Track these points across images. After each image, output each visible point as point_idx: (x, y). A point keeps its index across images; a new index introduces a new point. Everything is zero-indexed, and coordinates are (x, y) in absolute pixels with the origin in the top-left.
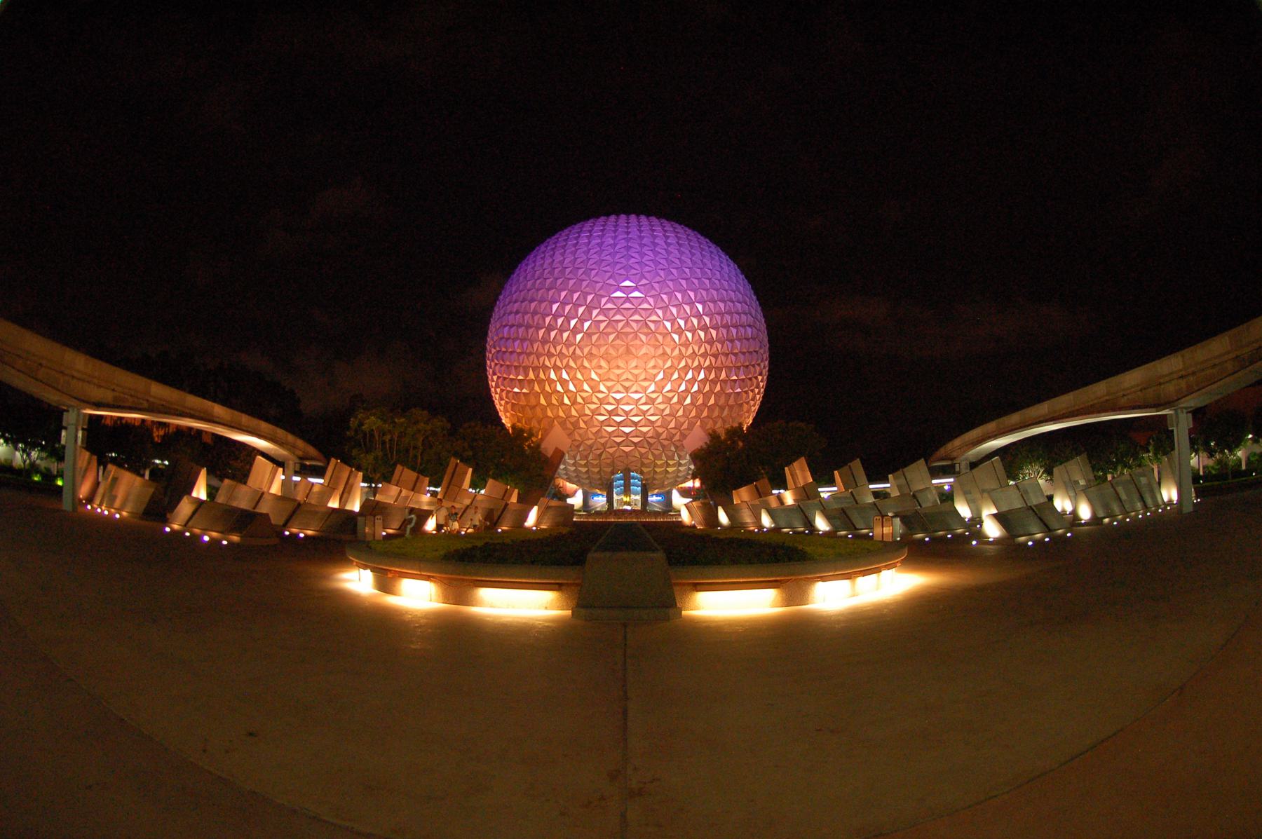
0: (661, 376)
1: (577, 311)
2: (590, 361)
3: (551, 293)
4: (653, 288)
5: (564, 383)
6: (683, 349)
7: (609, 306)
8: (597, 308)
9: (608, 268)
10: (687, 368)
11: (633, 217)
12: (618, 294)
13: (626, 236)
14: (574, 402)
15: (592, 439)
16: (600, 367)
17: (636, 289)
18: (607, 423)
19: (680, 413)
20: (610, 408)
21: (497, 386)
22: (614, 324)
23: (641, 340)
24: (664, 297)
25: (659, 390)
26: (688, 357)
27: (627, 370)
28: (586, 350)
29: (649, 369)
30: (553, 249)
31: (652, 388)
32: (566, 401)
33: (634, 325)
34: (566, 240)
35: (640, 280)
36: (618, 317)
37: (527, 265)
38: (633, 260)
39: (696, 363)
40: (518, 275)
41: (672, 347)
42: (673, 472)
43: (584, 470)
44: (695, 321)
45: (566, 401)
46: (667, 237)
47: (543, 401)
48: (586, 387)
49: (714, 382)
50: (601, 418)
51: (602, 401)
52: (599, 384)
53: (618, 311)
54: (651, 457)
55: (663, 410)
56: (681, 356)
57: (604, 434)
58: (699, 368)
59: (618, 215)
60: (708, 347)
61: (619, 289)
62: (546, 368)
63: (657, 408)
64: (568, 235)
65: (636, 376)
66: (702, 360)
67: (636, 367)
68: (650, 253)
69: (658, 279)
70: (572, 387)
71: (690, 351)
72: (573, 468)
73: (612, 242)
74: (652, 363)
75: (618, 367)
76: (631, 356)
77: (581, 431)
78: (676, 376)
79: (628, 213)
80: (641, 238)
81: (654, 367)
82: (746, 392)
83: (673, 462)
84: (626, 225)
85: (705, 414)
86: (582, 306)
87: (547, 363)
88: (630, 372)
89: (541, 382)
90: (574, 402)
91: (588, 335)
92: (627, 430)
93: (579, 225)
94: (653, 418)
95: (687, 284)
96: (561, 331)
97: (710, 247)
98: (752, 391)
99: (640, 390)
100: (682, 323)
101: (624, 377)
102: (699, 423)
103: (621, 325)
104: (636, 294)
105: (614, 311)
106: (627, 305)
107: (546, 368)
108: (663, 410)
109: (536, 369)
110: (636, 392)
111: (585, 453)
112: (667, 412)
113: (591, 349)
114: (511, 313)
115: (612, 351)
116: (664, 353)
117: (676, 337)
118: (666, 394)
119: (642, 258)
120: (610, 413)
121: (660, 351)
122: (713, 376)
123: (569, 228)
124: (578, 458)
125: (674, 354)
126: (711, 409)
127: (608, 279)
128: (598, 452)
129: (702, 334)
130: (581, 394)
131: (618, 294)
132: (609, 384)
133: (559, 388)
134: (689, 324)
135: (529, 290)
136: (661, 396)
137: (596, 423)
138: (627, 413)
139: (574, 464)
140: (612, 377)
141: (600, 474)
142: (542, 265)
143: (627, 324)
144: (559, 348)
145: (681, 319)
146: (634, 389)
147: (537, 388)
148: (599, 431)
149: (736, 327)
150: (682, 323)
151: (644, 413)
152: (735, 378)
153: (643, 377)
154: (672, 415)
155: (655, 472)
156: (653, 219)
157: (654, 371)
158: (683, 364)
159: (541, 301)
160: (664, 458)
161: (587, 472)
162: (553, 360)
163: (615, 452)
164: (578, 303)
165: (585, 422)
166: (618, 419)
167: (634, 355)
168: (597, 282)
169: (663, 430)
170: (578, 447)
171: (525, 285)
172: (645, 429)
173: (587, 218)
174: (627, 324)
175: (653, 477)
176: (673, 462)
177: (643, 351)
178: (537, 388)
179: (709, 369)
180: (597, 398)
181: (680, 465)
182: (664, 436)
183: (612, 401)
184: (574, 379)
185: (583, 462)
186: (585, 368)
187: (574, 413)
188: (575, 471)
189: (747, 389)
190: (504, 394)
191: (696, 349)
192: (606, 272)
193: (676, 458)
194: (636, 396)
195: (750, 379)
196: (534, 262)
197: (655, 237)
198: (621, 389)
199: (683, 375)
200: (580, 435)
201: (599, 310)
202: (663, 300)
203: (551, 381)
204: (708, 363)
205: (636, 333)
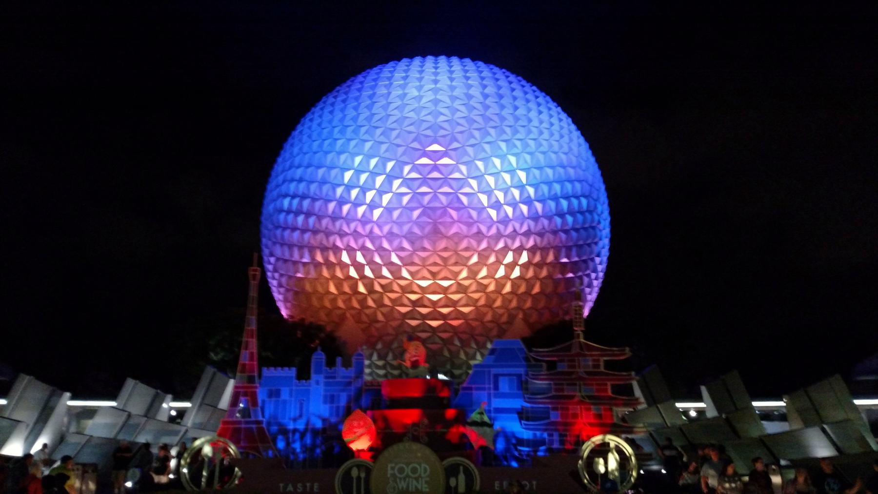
0: (475, 259)
2: (390, 242)
3: (343, 157)
4: (466, 153)
5: (359, 268)
6: (501, 227)
7: (414, 175)
8: (398, 178)
9: (411, 128)
10: (506, 249)
11: (442, 60)
13: (434, 86)
14: (371, 290)
16: (403, 249)
17: (445, 154)
18: (411, 315)
20: (414, 297)
21: (275, 270)
22: (419, 197)
23: (452, 217)
24: (480, 164)
25: (473, 274)
26: (508, 236)
27: (435, 252)
28: (386, 229)
29: (461, 250)
30: (344, 101)
31: (464, 274)
32: (362, 289)
33: (443, 199)
34: (359, 90)
35: (450, 144)
36: (424, 189)
37: (311, 120)
38: (442, 118)
39: (517, 244)
40: (301, 132)
41: (489, 224)
44: (516, 193)
45: (362, 289)
46: (485, 87)
48: (385, 272)
49: (539, 266)
50: (404, 310)
51: (406, 290)
53: (425, 181)
54: (463, 356)
56: (499, 236)
58: (520, 250)
59: (424, 56)
60: (532, 223)
62: (337, 250)
64: (361, 83)
65: (445, 260)
66: (524, 239)
67: (446, 249)
68: (463, 108)
69: (472, 141)
70: (368, 272)
71: (510, 229)
73: (415, 93)
74: (464, 244)
75: (424, 249)
77: (378, 325)
78: (492, 259)
79: (436, 54)
80: (452, 88)
81: (467, 249)
82: (580, 278)
84: (434, 70)
85: (528, 304)
86: (380, 174)
87: (339, 243)
88: (438, 255)
89: (330, 265)
90: (371, 290)
91: (389, 210)
92: (434, 323)
93: (375, 70)
95: (507, 146)
96: (356, 205)
97: (537, 97)
98: (588, 276)
99: (450, 276)
101: (431, 261)
102: (521, 316)
103: (427, 199)
104: (446, 161)
105: (420, 181)
106: (435, 175)
107: (337, 250)
108: (477, 300)
109: (324, 249)
110: (446, 278)
113: (391, 228)
114: (292, 180)
115: (416, 230)
116: (479, 232)
117: (493, 213)
118: (481, 281)
119: (453, 115)
120: (415, 303)
121: (474, 230)
123: (364, 74)
125: (490, 234)
126: (535, 298)
127: (412, 142)
129: (524, 208)
130: (379, 280)
131: (425, 161)
132: (413, 269)
133: (353, 273)
134: (509, 197)
135: (315, 153)
137: (396, 315)
138: (434, 304)
140: (417, 260)
142: (330, 122)
143: (435, 197)
144: (353, 225)
146: (442, 275)
148: (400, 326)
149: (567, 198)
150: (500, 196)
151: (454, 304)
152: (565, 260)
153: (452, 261)
154: (489, 305)
156: (467, 61)
157: (466, 254)
158: (501, 245)
159: (331, 168)
161: (385, 376)
162: (345, 239)
164: (376, 171)
167: (443, 235)
168: (399, 146)
169: (477, 323)
171: (310, 146)
172: (455, 323)
173: (386, 61)
174: (435, 197)
177: (454, 230)
178: (325, 273)
179: (532, 251)
180: (399, 285)
183: (416, 289)
184: (371, 263)
185: (380, 363)
186: (385, 250)
187: (370, 303)
189: (580, 274)
190: (284, 280)
191: (517, 226)
192: (410, 132)
194: (445, 283)
195: (585, 261)
196: (320, 116)
197: (469, 87)
198: (428, 275)
199: (501, 257)
202: (477, 168)
203: (344, 266)
204: (531, 243)
205: (444, 208)
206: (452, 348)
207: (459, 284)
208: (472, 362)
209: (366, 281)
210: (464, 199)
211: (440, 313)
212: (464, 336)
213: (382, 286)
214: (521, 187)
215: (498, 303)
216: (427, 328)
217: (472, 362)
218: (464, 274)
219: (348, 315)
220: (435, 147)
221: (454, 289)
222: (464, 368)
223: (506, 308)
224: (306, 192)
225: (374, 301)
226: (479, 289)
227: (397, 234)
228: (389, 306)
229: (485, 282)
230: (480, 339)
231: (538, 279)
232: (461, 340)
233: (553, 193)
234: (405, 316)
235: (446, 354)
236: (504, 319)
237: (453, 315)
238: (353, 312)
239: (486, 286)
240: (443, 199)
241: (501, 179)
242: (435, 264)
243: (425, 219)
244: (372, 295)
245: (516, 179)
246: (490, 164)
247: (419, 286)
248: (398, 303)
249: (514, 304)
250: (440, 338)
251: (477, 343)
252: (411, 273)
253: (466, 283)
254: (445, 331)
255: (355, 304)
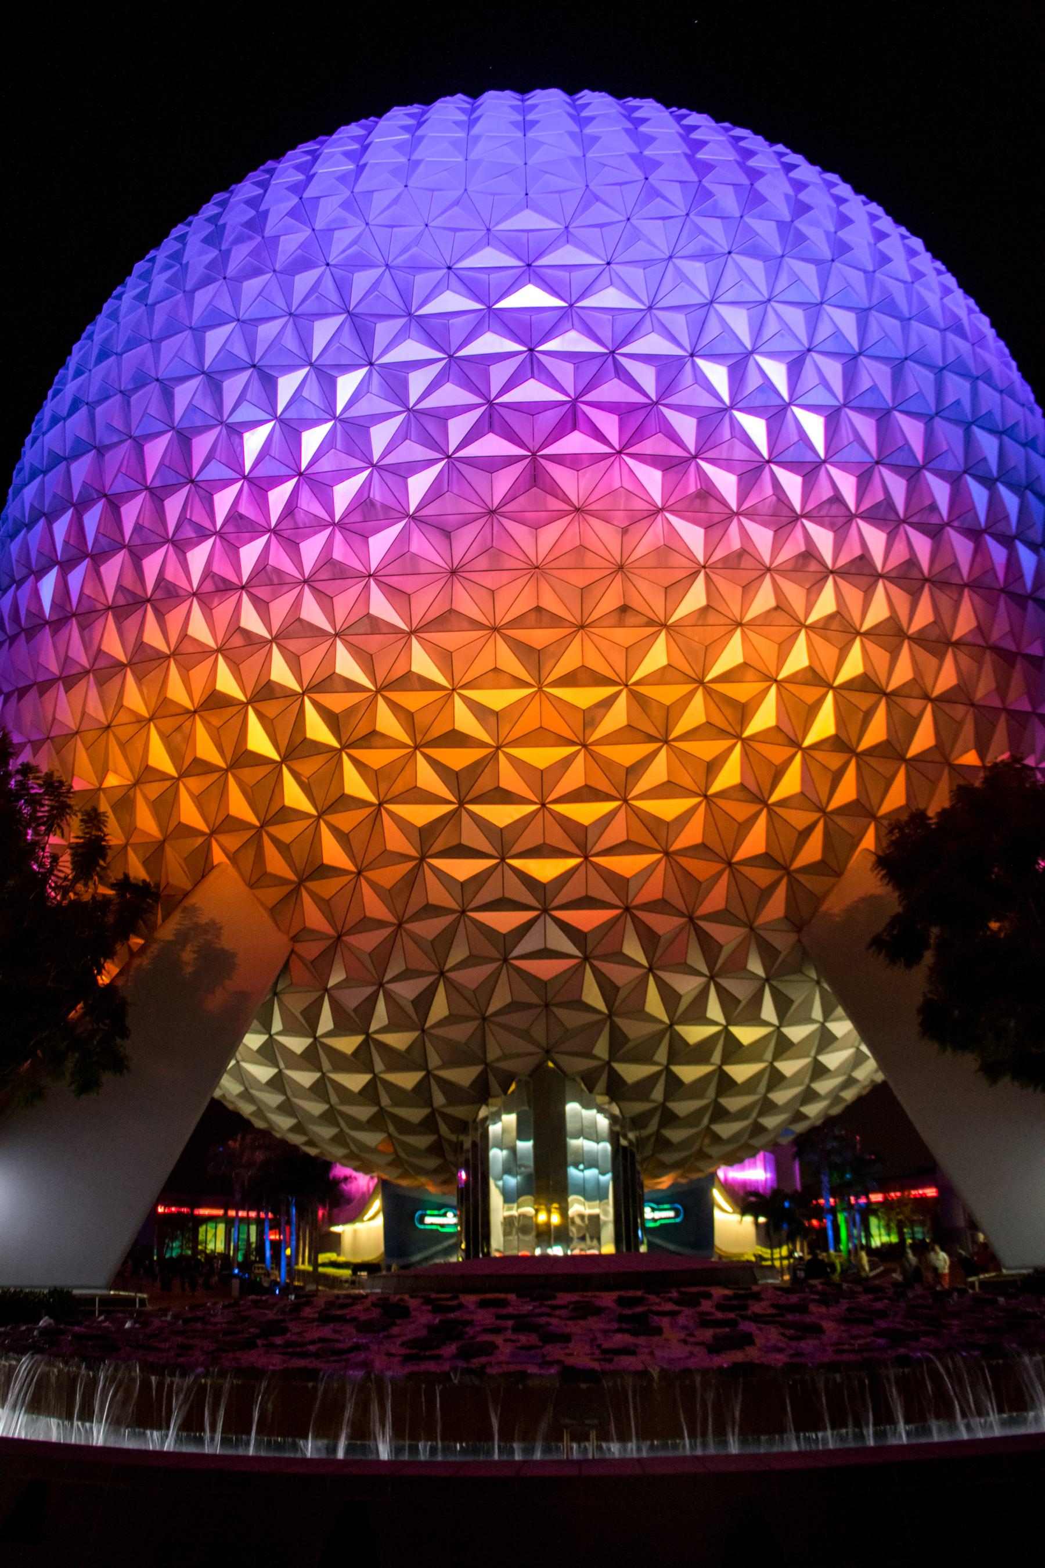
1: (305, 341)
12: (490, 257)
15: (381, 924)
17: (567, 236)
19: (790, 784)
20: (458, 759)
42: (751, 1084)
43: (355, 1082)
44: (833, 370)
45: (259, 741)
47: (160, 758)
48: (346, 665)
52: (408, 645)
54: (654, 1004)
55: (712, 768)
57: (438, 894)
61: (489, 238)
63: (683, 756)
72: (306, 1078)
76: (555, 504)
77: (328, 888)
83: (761, 1032)
94: (668, 809)
100: (777, 373)
102: (869, 841)
111: (353, 999)
112: (729, 775)
118: (721, 688)
122: (923, 616)
124: (326, 1022)
128: (407, 991)
131: (490, 257)
136: (699, 697)
137: (396, 841)
139: (310, 1059)
141: (429, 1103)
145: (771, 355)
147: (134, 699)
148: (412, 880)
155: (674, 1084)
160: (714, 1010)
161: (369, 1093)
163: (490, 985)
165: (343, 838)
166: (501, 815)
167: (566, 500)
170: (321, 966)
175: (664, 1107)
176: (761, 1032)
181: (784, 1047)
182: (716, 899)
185: (347, 1044)
187: (294, 795)
188: (319, 1090)
193: (768, 1011)
198: (511, 664)
200: (324, 905)
201: (402, 321)
206: (620, 974)
207: (639, 700)
208: (694, 1034)
209: (272, 709)
210: (646, 377)
211: (564, 821)
212: (663, 924)
213: (332, 720)
214: (851, 362)
215: (790, 784)
216: (518, 892)
217: (694, 1034)
218: (657, 657)
219: (218, 856)
220: (528, 220)
221: (617, 717)
222: (661, 1054)
223: (822, 810)
224: (83, 436)
225: (306, 788)
226: (719, 721)
227: (386, 508)
228: (365, 804)
229: (740, 692)
230: (727, 936)
231: (927, 697)
232: (649, 939)
233: (949, 399)
234: (426, 835)
235: (593, 995)
236: (812, 851)
237: (616, 833)
238: (233, 842)
239: (744, 711)
240: (565, 372)
241: (771, 317)
242: (540, 615)
243: (492, 445)
244: (297, 766)
245: (824, 331)
246: (730, 277)
247: (479, 711)
248: (399, 787)
249: (847, 791)
250: (568, 930)
251: (709, 947)
252: (445, 658)
253: (667, 694)
254: (587, 902)
255: (239, 806)
